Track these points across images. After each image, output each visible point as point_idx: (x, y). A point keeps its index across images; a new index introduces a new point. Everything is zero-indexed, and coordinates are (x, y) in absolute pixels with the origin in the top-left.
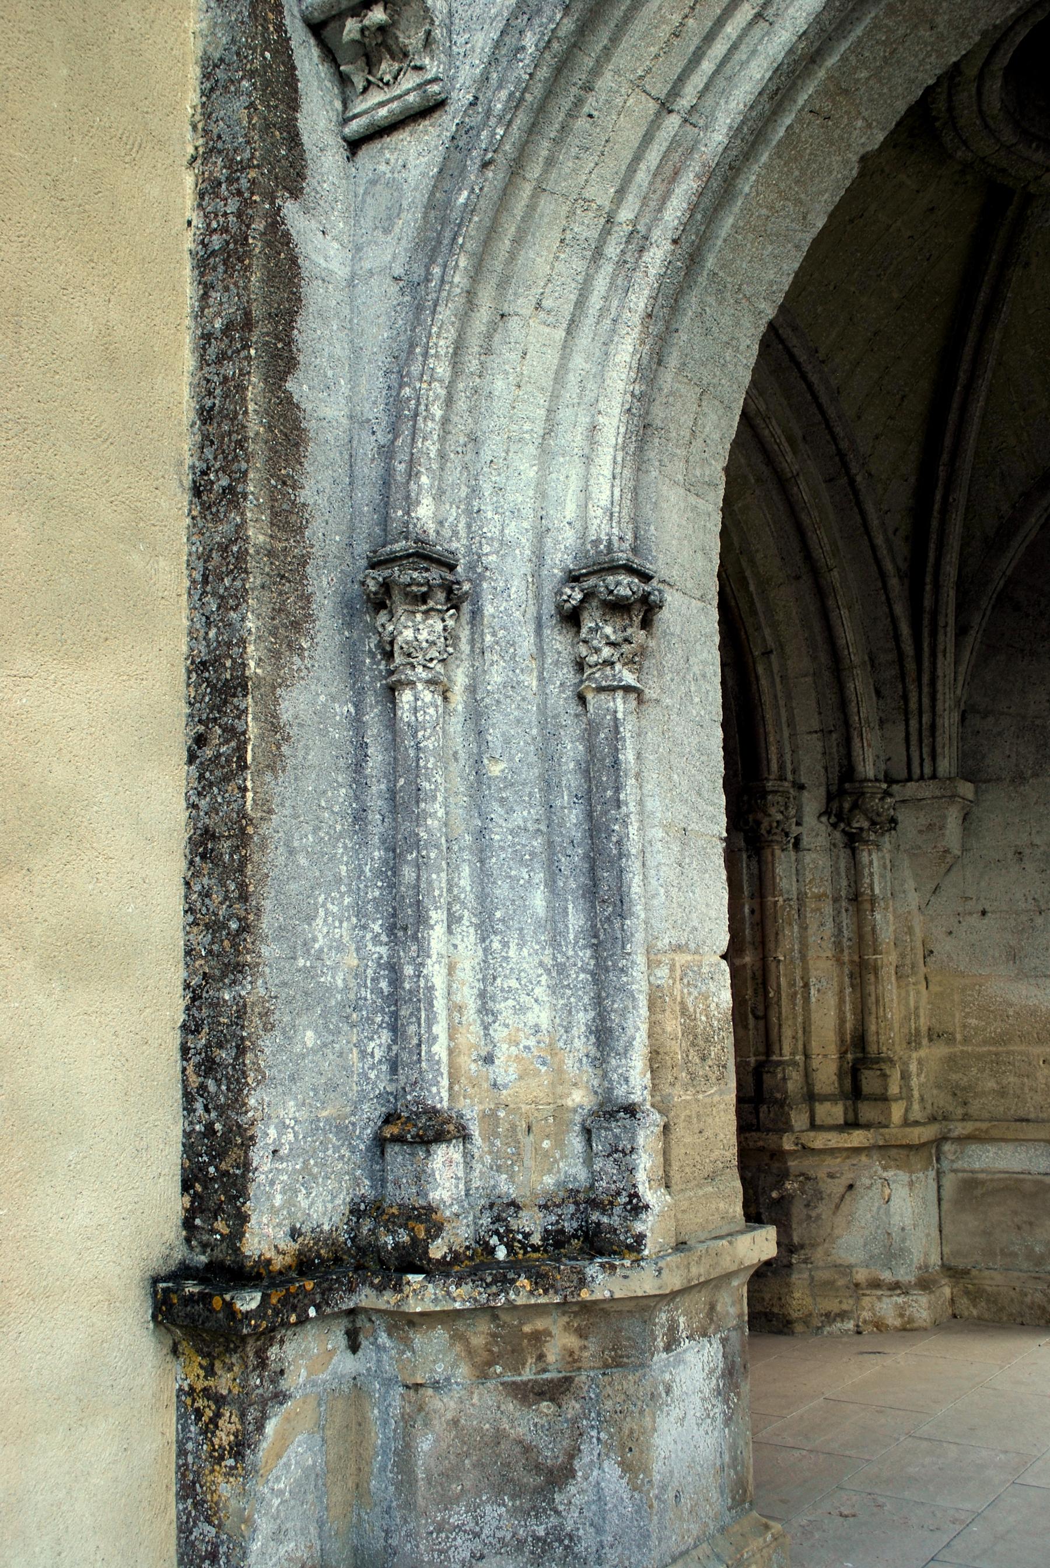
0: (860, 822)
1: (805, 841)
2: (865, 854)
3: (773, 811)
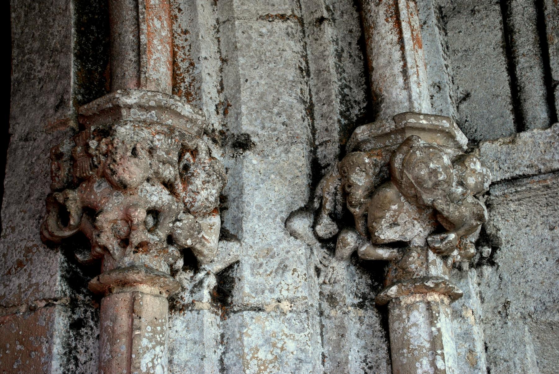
0: (400, 224)
1: (247, 287)
2: (418, 316)
3: (132, 171)
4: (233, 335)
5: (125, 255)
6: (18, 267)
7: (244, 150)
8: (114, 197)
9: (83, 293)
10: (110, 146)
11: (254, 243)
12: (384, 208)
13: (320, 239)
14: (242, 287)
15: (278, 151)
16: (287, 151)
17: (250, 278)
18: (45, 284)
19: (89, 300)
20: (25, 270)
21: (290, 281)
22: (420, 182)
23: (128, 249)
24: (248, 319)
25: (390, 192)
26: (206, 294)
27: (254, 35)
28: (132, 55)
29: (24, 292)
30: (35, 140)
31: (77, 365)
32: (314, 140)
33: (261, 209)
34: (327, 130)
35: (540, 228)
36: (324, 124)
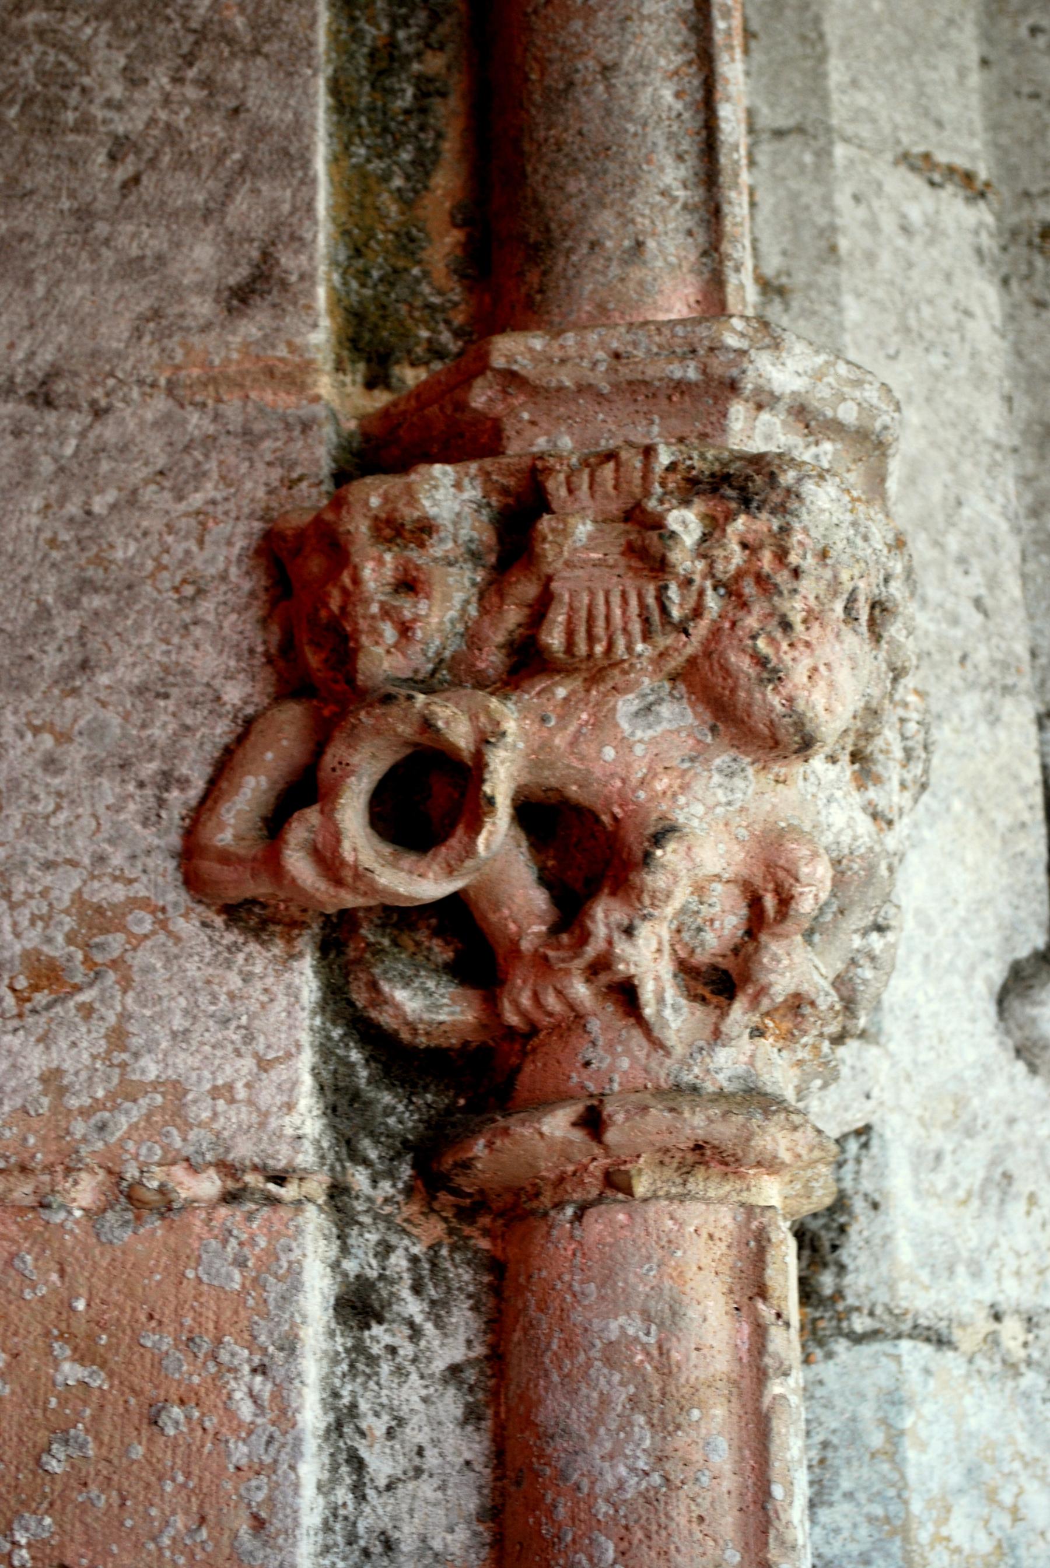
4: (855, 1437)
6: (35, 988)
8: (717, 778)
9: (366, 1162)
10: (766, 560)
11: (915, 1062)
14: (887, 1238)
19: (387, 1200)
20: (87, 1011)
21: (1022, 1242)
23: (739, 1013)
24: (915, 1376)
27: (888, 223)
28: (672, 174)
29: (85, 1113)
30: (99, 413)
31: (358, 1491)
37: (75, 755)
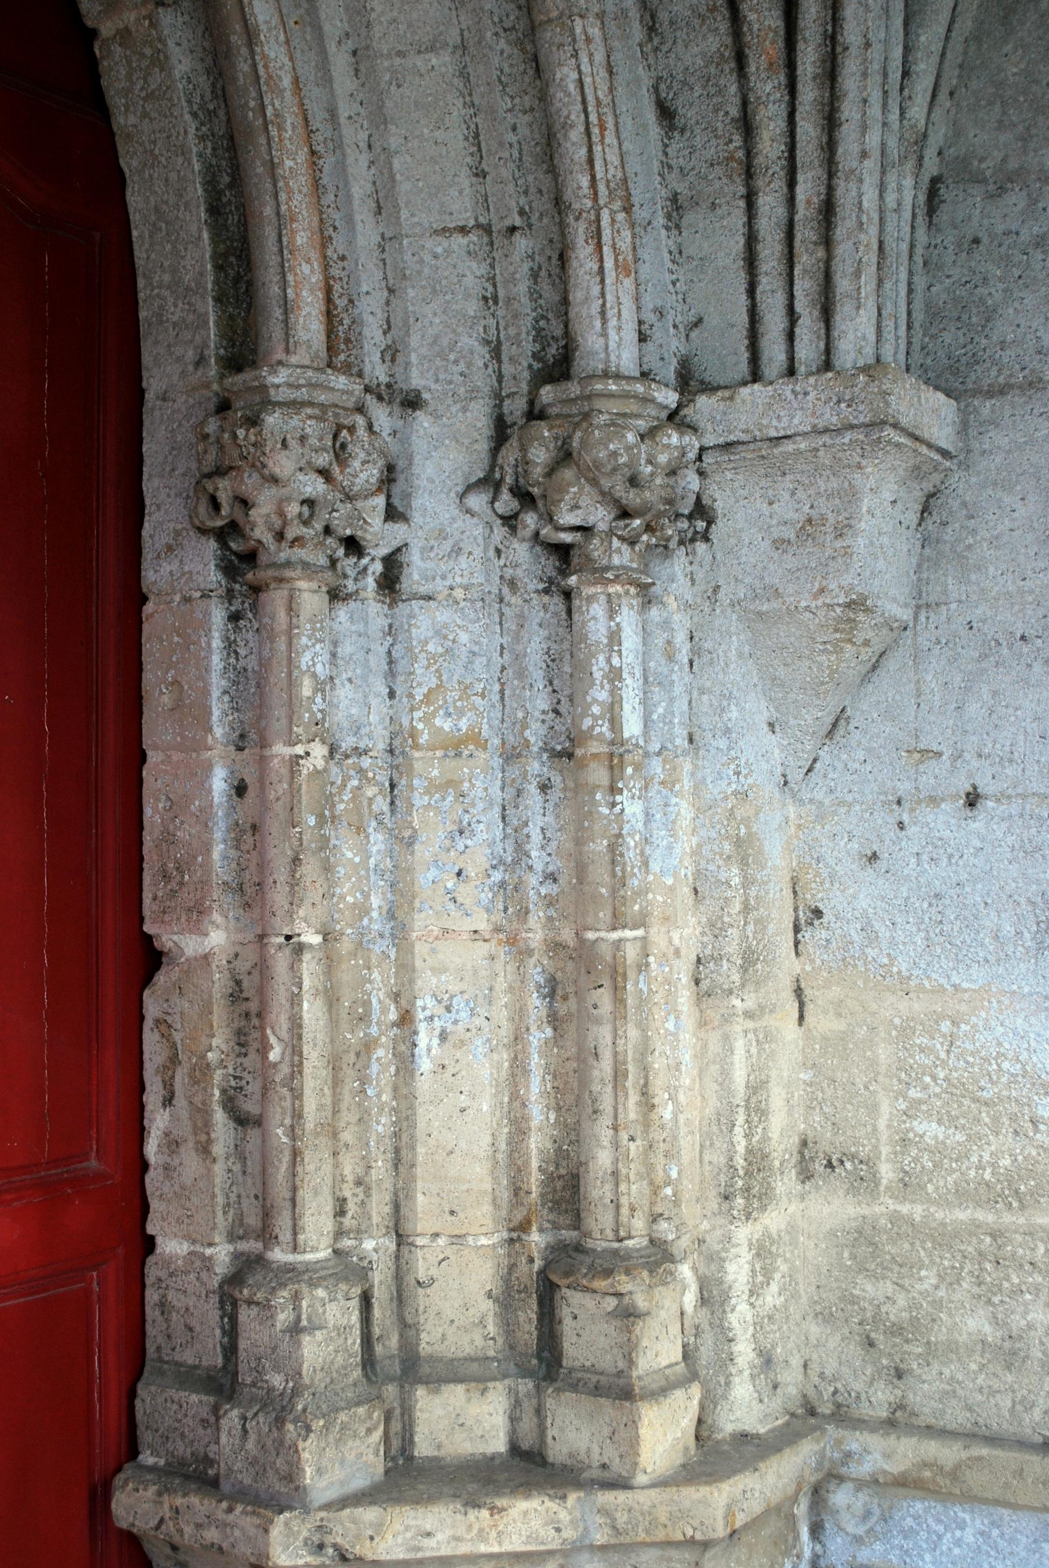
0: (580, 508)
1: (416, 573)
2: (598, 610)
3: (283, 464)
4: (402, 626)
5: (280, 551)
7: (414, 410)
12: (563, 490)
13: (501, 517)
15: (454, 409)
16: (464, 410)
17: (419, 563)
18: (198, 573)
21: (464, 566)
22: (598, 465)
23: (283, 544)
24: (417, 609)
25: (568, 473)
26: (370, 582)
27: (428, 258)
28: (278, 313)
31: (237, 659)
32: (501, 389)
33: (433, 482)
34: (515, 378)
35: (759, 501)
36: (512, 370)
37: (172, 493)
